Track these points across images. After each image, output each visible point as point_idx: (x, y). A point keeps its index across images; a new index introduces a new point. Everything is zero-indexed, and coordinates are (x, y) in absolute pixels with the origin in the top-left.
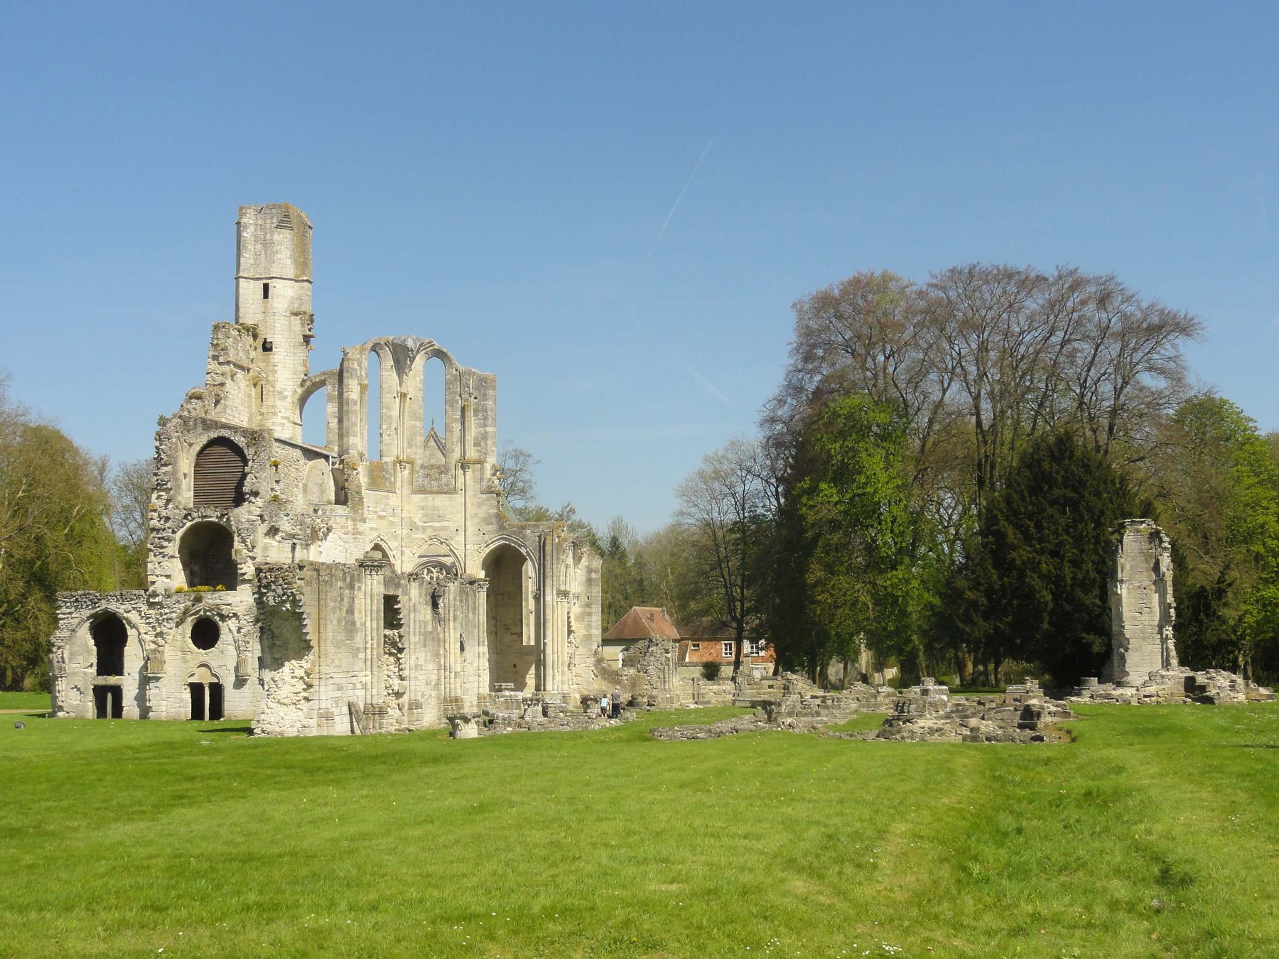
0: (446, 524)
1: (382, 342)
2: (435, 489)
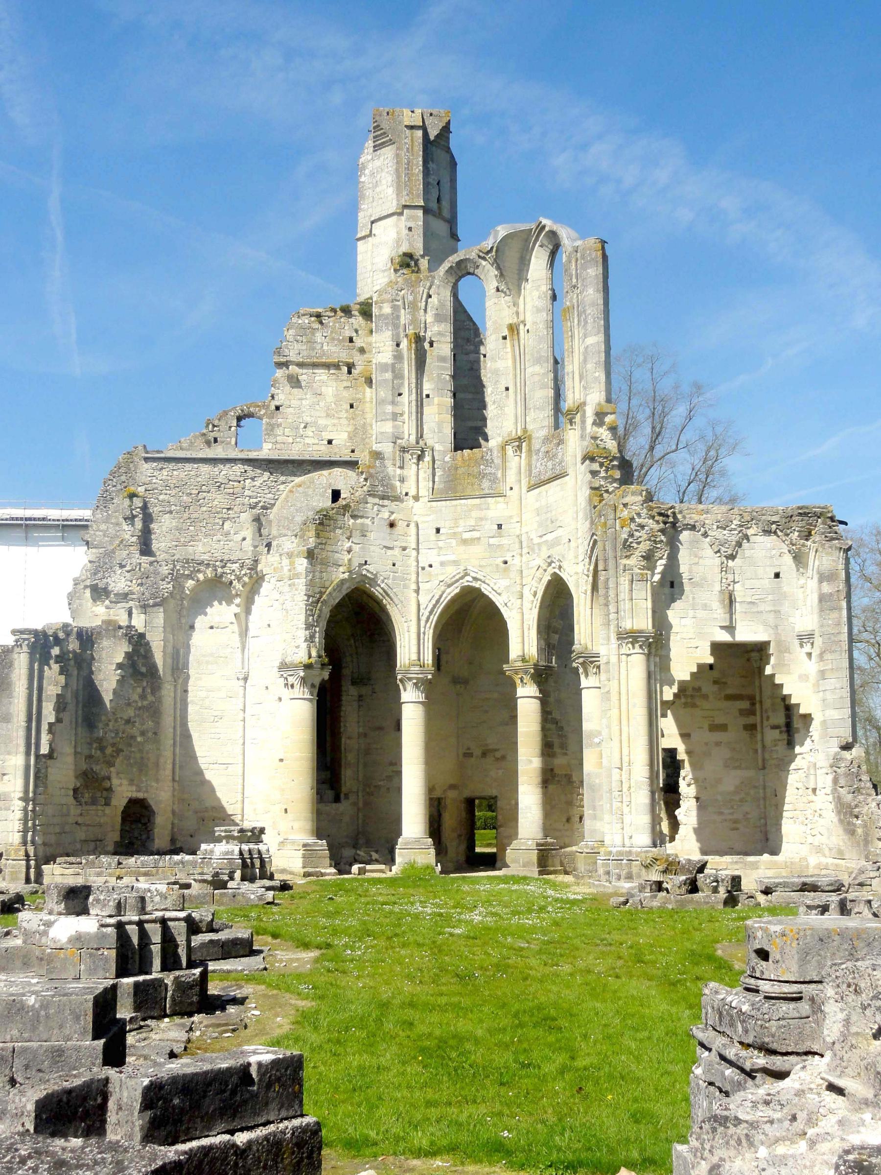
0: (559, 532)
1: (473, 255)
2: (549, 474)
